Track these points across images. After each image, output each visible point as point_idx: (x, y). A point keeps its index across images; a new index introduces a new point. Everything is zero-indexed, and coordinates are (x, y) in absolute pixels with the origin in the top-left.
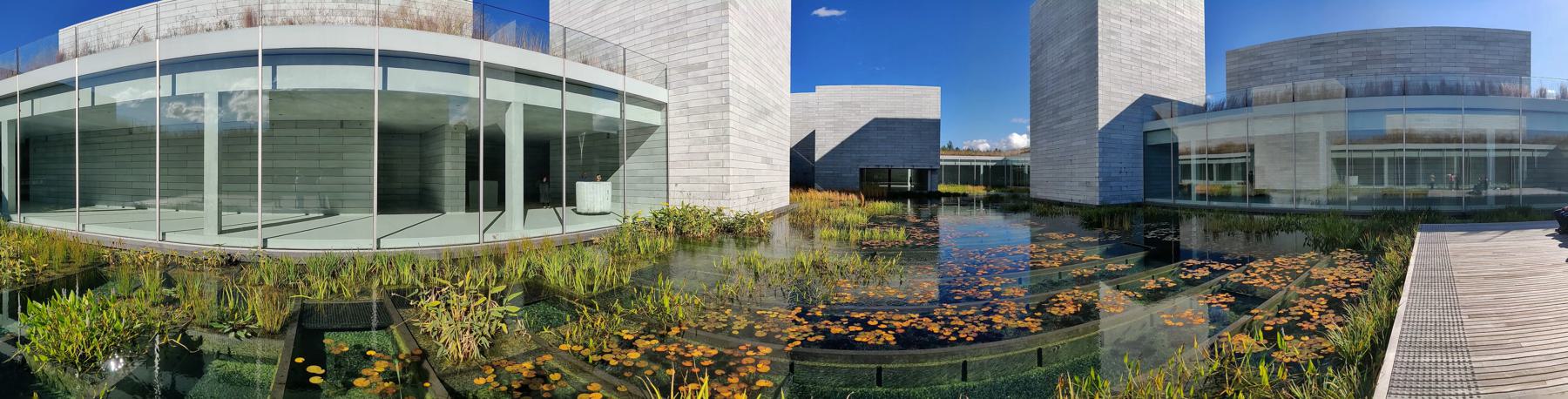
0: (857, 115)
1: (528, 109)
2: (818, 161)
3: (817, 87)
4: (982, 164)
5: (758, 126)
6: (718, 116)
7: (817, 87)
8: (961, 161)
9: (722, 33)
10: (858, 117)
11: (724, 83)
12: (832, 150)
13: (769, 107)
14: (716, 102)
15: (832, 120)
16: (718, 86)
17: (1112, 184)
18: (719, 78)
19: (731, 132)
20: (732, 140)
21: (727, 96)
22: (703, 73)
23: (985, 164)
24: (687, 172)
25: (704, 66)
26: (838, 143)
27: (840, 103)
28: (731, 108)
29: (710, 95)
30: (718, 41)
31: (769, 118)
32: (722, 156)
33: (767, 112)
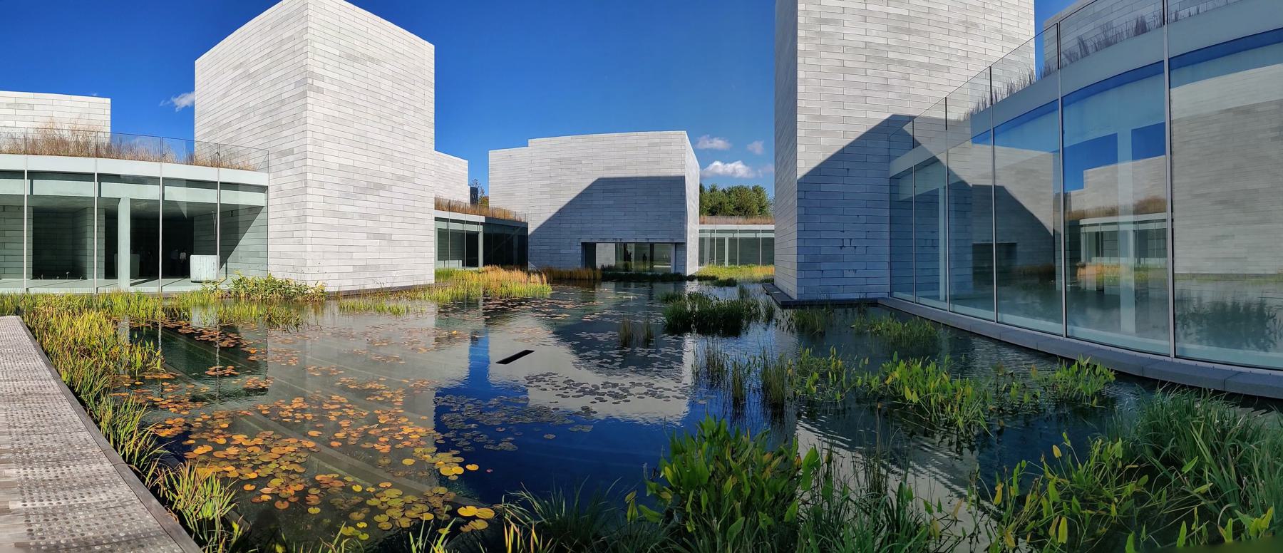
0: (579, 174)
2: (531, 235)
3: (530, 140)
4: (727, 236)
5: (357, 203)
6: (300, 198)
7: (530, 140)
8: (763, 231)
9: (303, 120)
10: (580, 177)
11: (304, 168)
12: (549, 220)
13: (383, 181)
15: (548, 182)
17: (825, 266)
18: (300, 163)
19: (308, 212)
20: (310, 220)
23: (731, 235)
26: (554, 211)
27: (559, 160)
29: (295, 179)
31: (382, 193)
33: (380, 187)
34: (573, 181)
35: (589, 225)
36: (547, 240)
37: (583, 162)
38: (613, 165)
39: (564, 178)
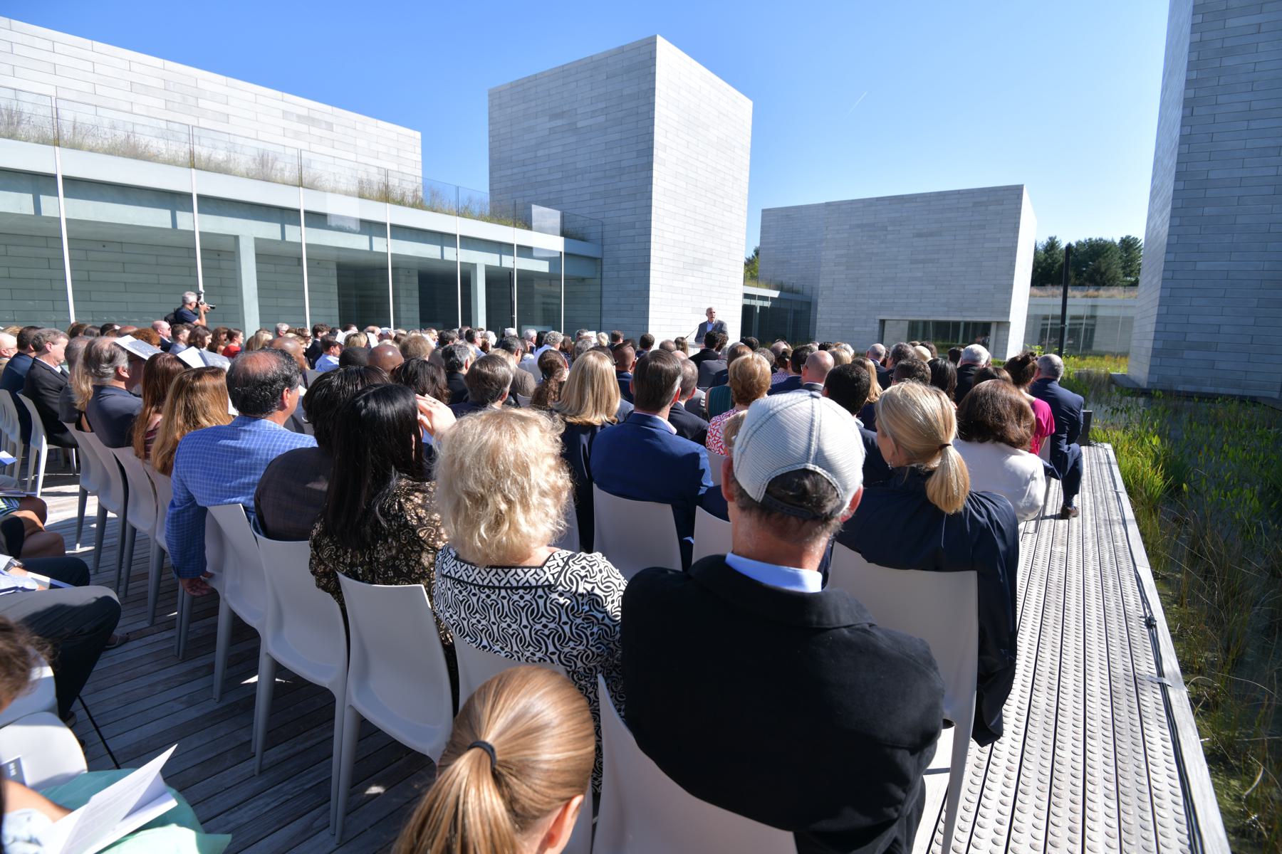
31: (706, 269)
35: (891, 301)
37: (889, 228)
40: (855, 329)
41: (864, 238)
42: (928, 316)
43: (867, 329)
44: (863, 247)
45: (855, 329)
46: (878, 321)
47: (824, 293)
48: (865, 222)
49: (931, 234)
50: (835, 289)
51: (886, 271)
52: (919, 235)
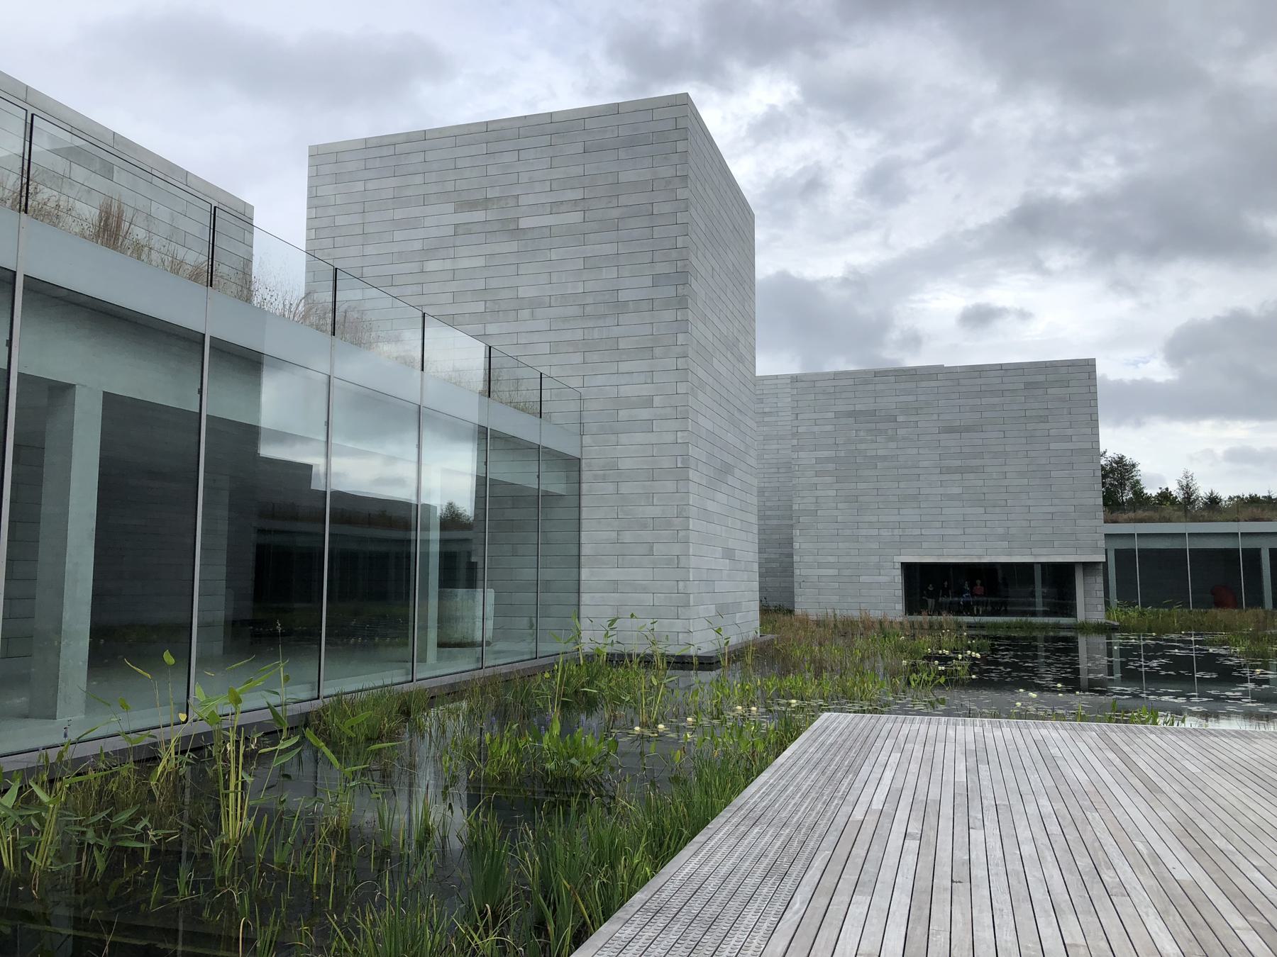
1: (111, 402)
6: (670, 486)
10: (893, 445)
14: (666, 463)
15: (831, 454)
16: (669, 438)
21: (686, 456)
22: (644, 414)
24: (614, 574)
25: (648, 402)
27: (853, 414)
28: (691, 474)
30: (670, 363)
32: (676, 549)
34: (881, 452)
35: (917, 532)
36: (831, 559)
37: (900, 419)
38: (957, 423)
39: (863, 446)
40: (862, 579)
41: (862, 433)
42: (979, 556)
43: (882, 579)
44: (859, 446)
45: (862, 579)
46: (899, 566)
47: (801, 519)
48: (858, 407)
49: (968, 429)
50: (819, 512)
51: (902, 485)
52: (950, 430)
